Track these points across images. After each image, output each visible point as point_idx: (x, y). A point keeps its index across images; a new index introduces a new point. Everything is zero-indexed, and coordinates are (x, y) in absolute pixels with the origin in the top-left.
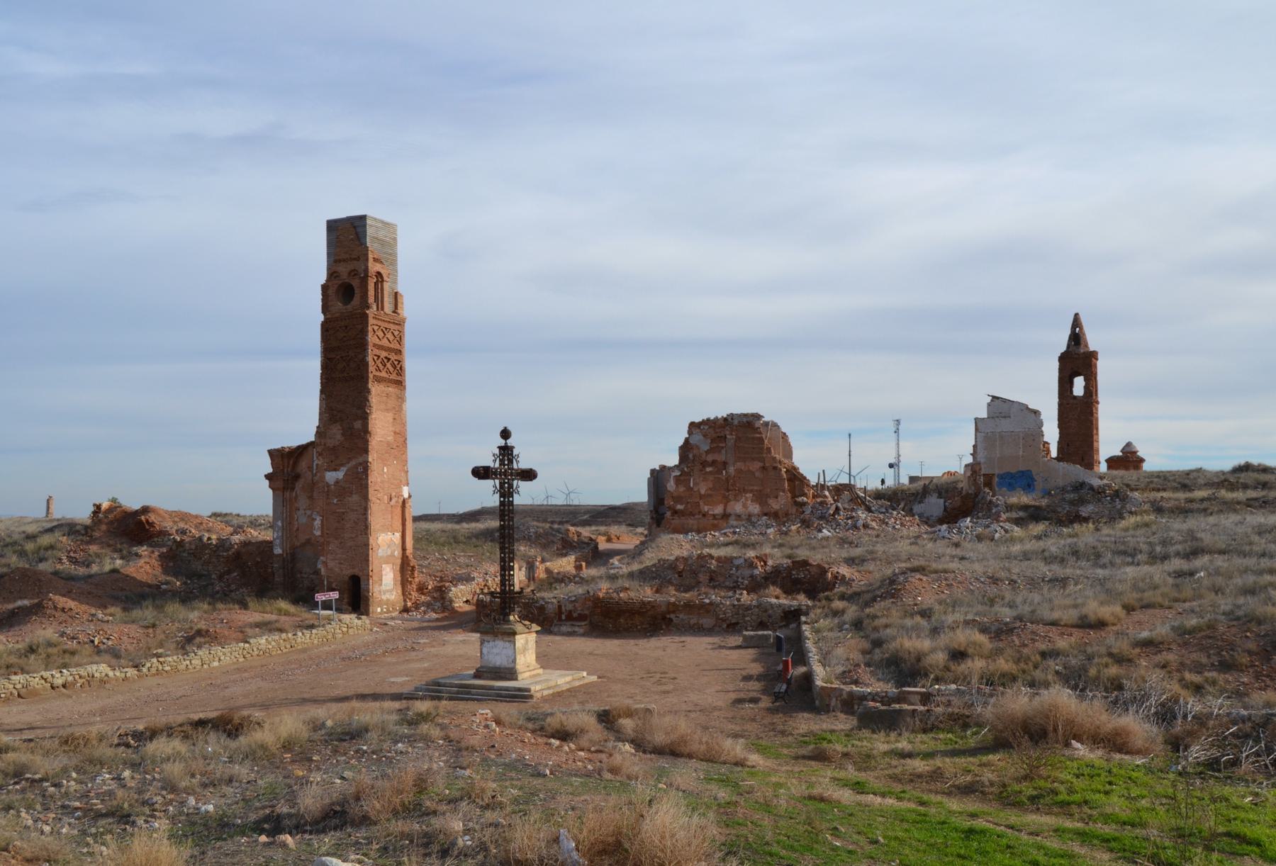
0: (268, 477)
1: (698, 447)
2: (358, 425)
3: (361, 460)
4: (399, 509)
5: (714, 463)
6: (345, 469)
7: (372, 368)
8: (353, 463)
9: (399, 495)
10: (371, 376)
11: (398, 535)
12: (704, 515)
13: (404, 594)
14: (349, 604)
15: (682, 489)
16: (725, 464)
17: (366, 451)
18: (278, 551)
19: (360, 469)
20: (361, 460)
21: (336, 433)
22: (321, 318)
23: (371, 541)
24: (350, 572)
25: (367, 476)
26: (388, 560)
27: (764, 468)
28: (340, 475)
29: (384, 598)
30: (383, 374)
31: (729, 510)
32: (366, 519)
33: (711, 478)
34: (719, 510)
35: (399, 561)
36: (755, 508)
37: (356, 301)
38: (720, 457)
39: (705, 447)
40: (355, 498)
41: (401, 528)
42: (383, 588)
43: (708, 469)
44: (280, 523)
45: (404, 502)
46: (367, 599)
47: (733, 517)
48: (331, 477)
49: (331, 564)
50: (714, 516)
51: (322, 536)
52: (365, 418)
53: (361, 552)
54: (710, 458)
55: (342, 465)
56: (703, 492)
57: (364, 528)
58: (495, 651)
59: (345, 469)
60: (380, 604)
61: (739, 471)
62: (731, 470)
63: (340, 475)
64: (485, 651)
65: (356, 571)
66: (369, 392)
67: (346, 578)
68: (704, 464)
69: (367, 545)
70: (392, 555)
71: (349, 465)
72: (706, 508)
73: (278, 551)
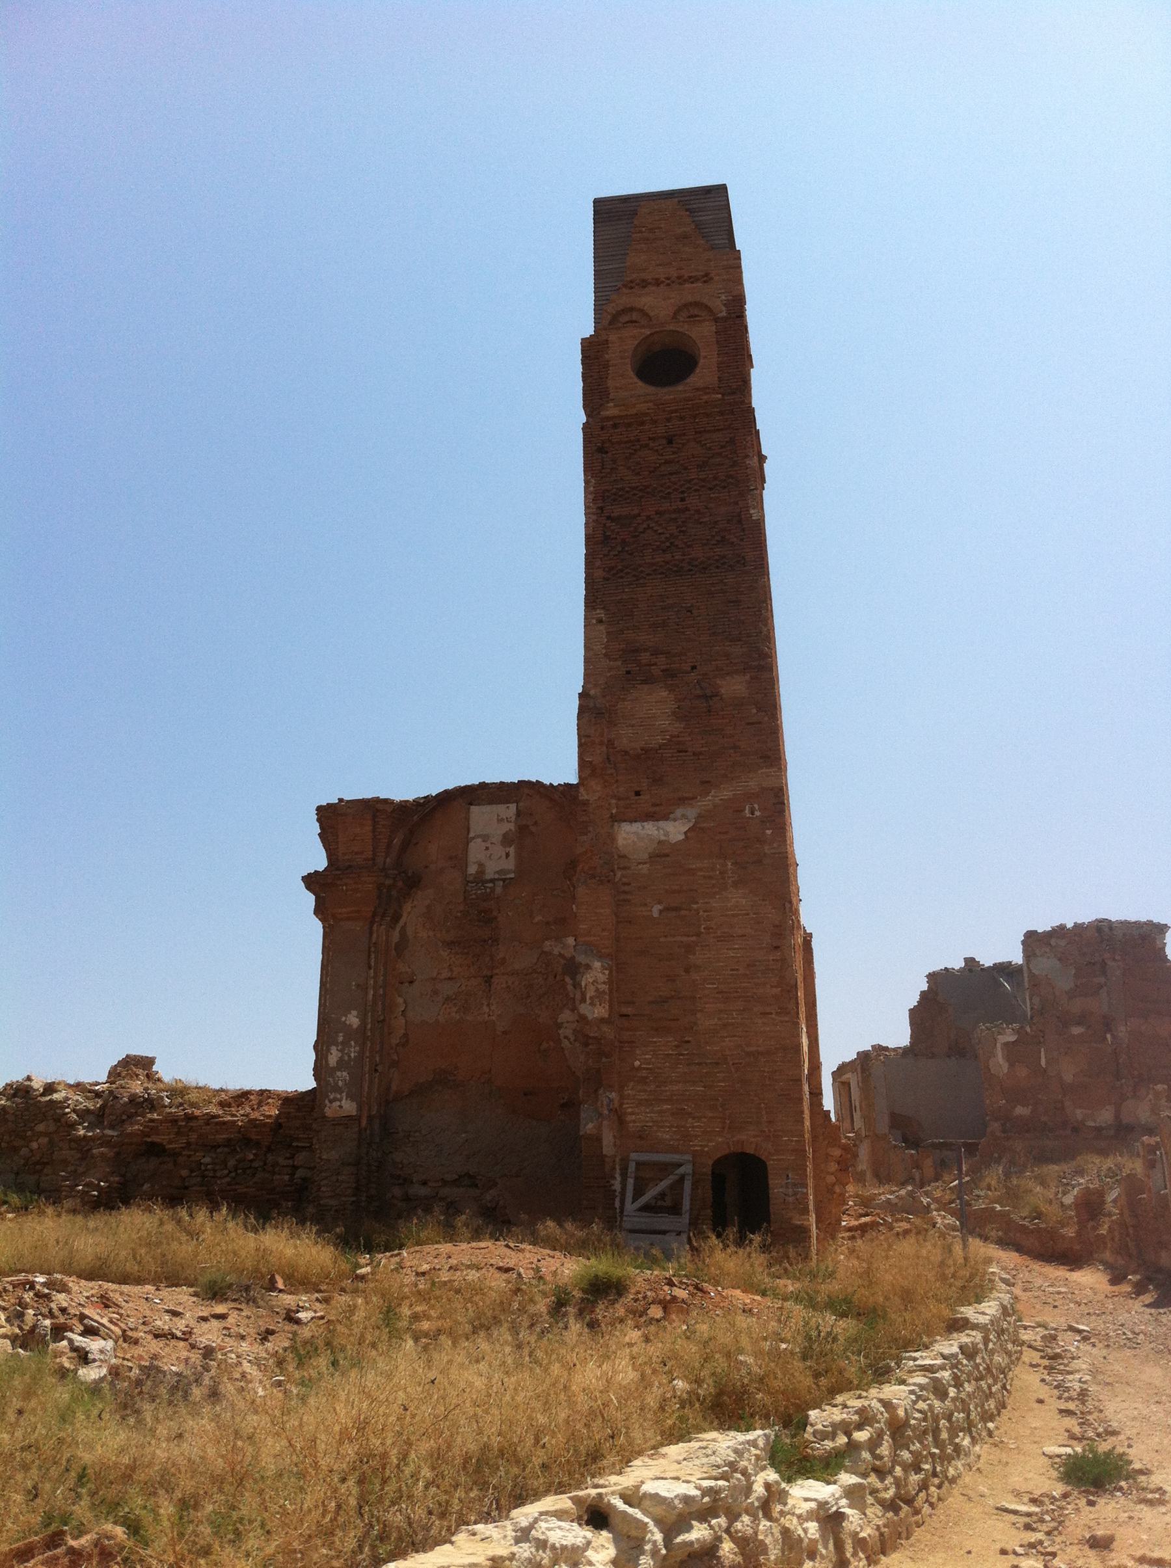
0: (311, 881)
2: (734, 686)
3: (753, 783)
6: (692, 812)
12: (1075, 1130)
15: (1022, 1072)
16: (1108, 1024)
20: (753, 783)
28: (675, 830)
34: (1105, 1116)
37: (705, 375)
39: (1065, 983)
43: (1076, 1030)
44: (353, 1020)
48: (635, 836)
49: (638, 1117)
50: (1098, 1129)
55: (683, 801)
56: (1068, 1078)
59: (692, 812)
62: (1122, 1031)
65: (750, 1140)
71: (706, 802)
72: (1079, 1113)
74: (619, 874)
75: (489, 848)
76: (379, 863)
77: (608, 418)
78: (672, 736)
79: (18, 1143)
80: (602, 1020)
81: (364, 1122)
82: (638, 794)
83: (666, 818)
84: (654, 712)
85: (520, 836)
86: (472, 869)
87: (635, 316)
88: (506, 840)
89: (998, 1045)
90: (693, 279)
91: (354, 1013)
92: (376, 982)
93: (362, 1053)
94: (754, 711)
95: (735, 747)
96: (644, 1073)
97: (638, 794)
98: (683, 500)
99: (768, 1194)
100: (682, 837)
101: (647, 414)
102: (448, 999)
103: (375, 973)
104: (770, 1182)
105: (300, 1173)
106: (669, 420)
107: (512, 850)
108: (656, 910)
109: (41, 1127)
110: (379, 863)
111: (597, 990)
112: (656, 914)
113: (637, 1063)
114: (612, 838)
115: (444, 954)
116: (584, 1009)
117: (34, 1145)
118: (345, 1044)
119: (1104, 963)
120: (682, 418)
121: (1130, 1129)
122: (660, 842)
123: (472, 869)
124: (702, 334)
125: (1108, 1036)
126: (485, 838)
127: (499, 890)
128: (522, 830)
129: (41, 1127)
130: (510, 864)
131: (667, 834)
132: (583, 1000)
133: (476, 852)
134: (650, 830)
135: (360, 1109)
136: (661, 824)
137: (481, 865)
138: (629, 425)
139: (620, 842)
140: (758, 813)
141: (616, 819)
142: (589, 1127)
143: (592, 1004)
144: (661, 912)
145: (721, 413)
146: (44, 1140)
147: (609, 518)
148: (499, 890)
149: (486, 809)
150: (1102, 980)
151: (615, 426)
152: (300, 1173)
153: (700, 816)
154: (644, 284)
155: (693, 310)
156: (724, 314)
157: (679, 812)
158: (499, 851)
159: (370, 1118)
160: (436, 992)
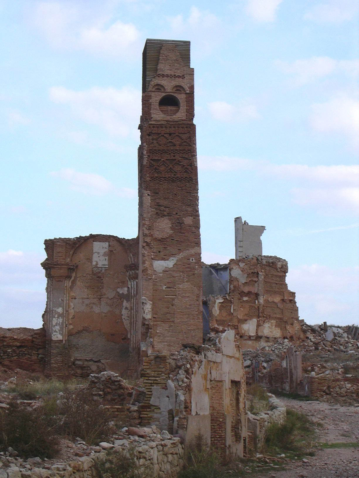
0: (44, 265)
1: (237, 280)
2: (188, 220)
5: (249, 294)
16: (257, 295)
20: (192, 251)
21: (164, 227)
27: (283, 300)
28: (170, 263)
31: (260, 334)
33: (247, 306)
36: (277, 333)
38: (254, 290)
39: (243, 280)
43: (245, 299)
47: (263, 338)
48: (160, 265)
49: (158, 346)
54: (246, 289)
55: (173, 255)
61: (267, 301)
62: (261, 300)
63: (170, 263)
68: (243, 294)
74: (154, 276)
75: (99, 257)
76: (64, 259)
77: (151, 124)
82: (159, 252)
83: (168, 260)
84: (164, 227)
85: (111, 253)
86: (94, 263)
87: (159, 87)
88: (105, 254)
89: (216, 303)
90: (179, 77)
95: (188, 240)
97: (159, 252)
98: (174, 156)
101: (163, 125)
102: (87, 305)
105: (40, 356)
106: (170, 127)
107: (107, 258)
108: (164, 287)
110: (64, 259)
113: (158, 331)
114: (152, 265)
115: (86, 290)
116: (145, 315)
118: (58, 317)
119: (258, 273)
120: (174, 127)
121: (261, 337)
122: (166, 267)
123: (94, 263)
124: (181, 97)
125: (257, 301)
126: (98, 253)
127: (103, 271)
128: (111, 251)
130: (106, 263)
132: (144, 312)
133: (95, 258)
134: (162, 263)
136: (166, 261)
137: (97, 262)
138: (158, 127)
140: (194, 261)
142: (144, 349)
145: (186, 127)
147: (151, 160)
148: (103, 271)
149: (98, 243)
150: (256, 279)
151: (153, 127)
152: (40, 356)
153: (177, 261)
154: (163, 76)
155: (179, 88)
156: (188, 92)
157: (172, 258)
158: (102, 258)
160: (83, 302)
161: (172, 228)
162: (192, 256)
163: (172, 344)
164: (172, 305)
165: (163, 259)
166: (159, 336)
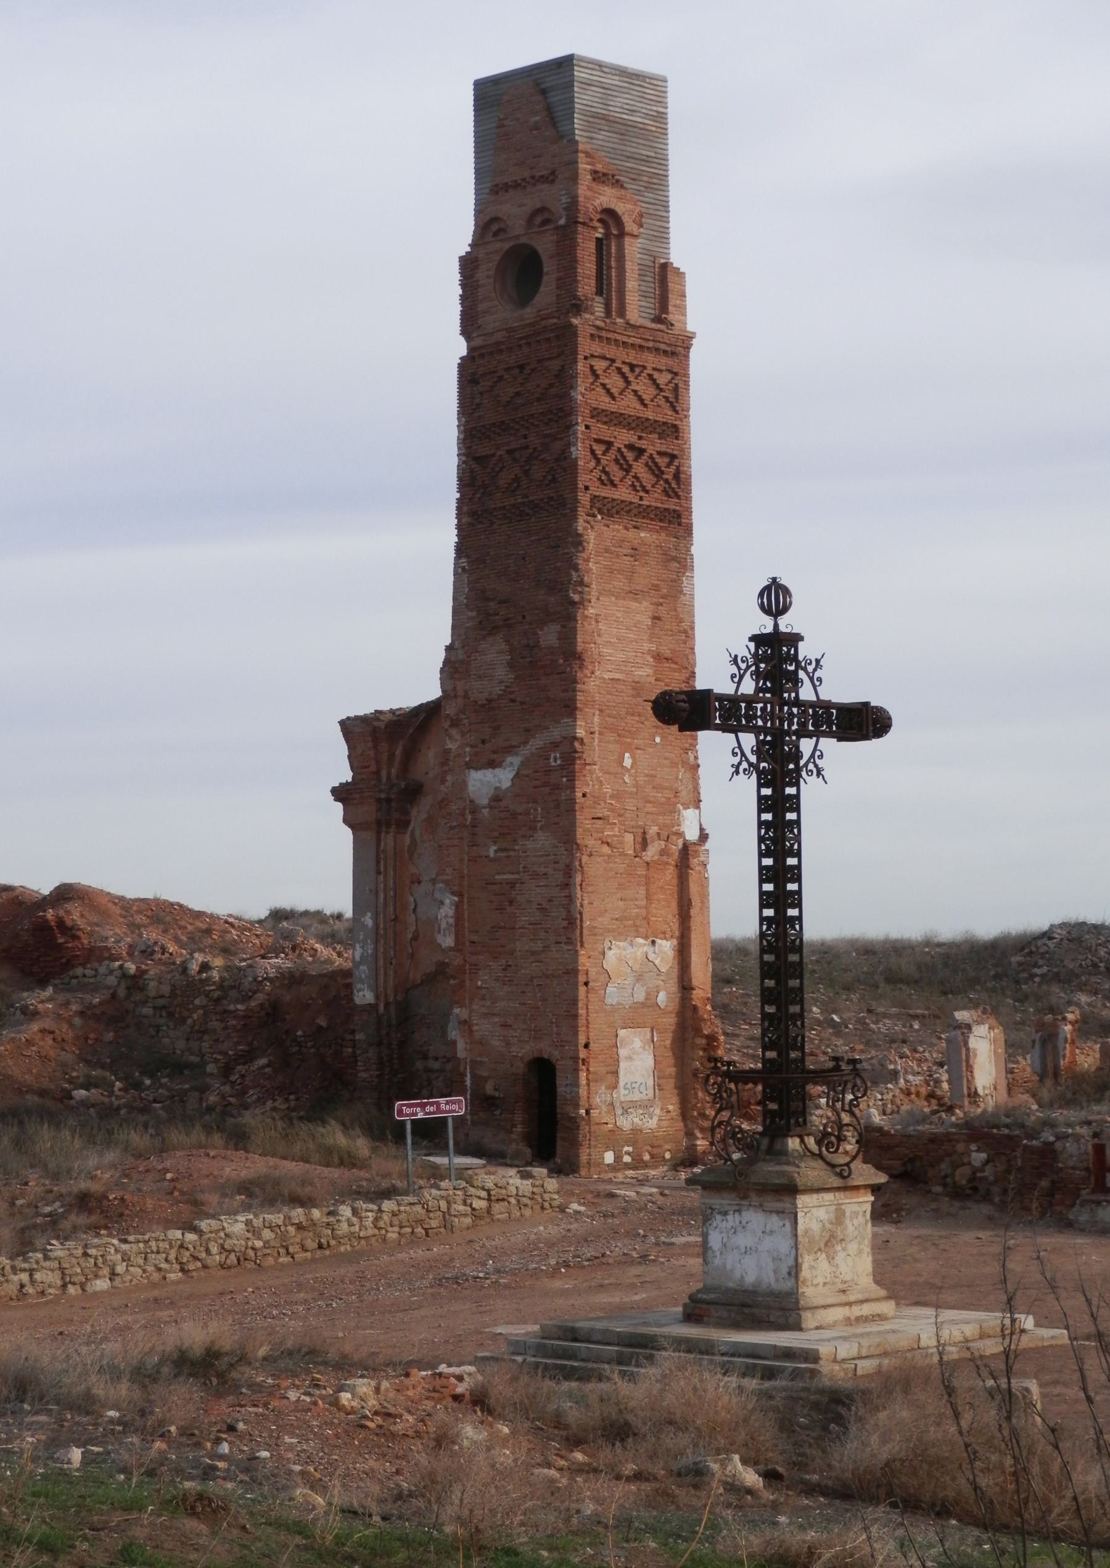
4: (669, 875)
7: (587, 476)
8: (537, 742)
9: (672, 833)
10: (584, 498)
11: (667, 947)
13: (684, 1115)
14: (527, 1138)
17: (570, 709)
18: (364, 996)
19: (555, 760)
20: (556, 733)
22: (461, 348)
23: (584, 962)
24: (527, 1050)
25: (572, 779)
26: (637, 1016)
28: (503, 777)
29: (625, 1123)
30: (623, 493)
32: (570, 898)
35: (670, 1021)
40: (543, 840)
41: (675, 926)
42: (622, 1094)
45: (686, 847)
46: (574, 1124)
49: (483, 1028)
51: (458, 947)
52: (566, 614)
53: (560, 990)
57: (568, 928)
58: (743, 1240)
60: (614, 1139)
63: (503, 777)
64: (715, 1240)
65: (546, 1049)
66: (578, 542)
67: (520, 1068)
69: (572, 972)
70: (650, 1003)
71: (526, 751)
73: (364, 996)
78: (507, 687)
79: (185, 1013)
80: (450, 949)
81: (381, 1009)
91: (369, 914)
92: (385, 886)
93: (376, 949)
94: (561, 661)
96: (484, 991)
97: (483, 742)
99: (556, 1092)
100: (509, 784)
103: (385, 877)
104: (558, 1082)
109: (197, 1002)
111: (447, 923)
112: (492, 855)
113: (479, 983)
114: (464, 785)
117: (195, 1016)
122: (497, 788)
129: (197, 1002)
131: (500, 781)
135: (377, 997)
136: (497, 771)
139: (471, 788)
140: (559, 762)
141: (469, 766)
143: (444, 935)
144: (496, 851)
146: (201, 1012)
157: (509, 759)
159: (387, 1005)
161: (511, 665)
162: (555, 745)
163: (509, 1022)
164: (511, 902)
165: (492, 764)
166: (483, 998)
